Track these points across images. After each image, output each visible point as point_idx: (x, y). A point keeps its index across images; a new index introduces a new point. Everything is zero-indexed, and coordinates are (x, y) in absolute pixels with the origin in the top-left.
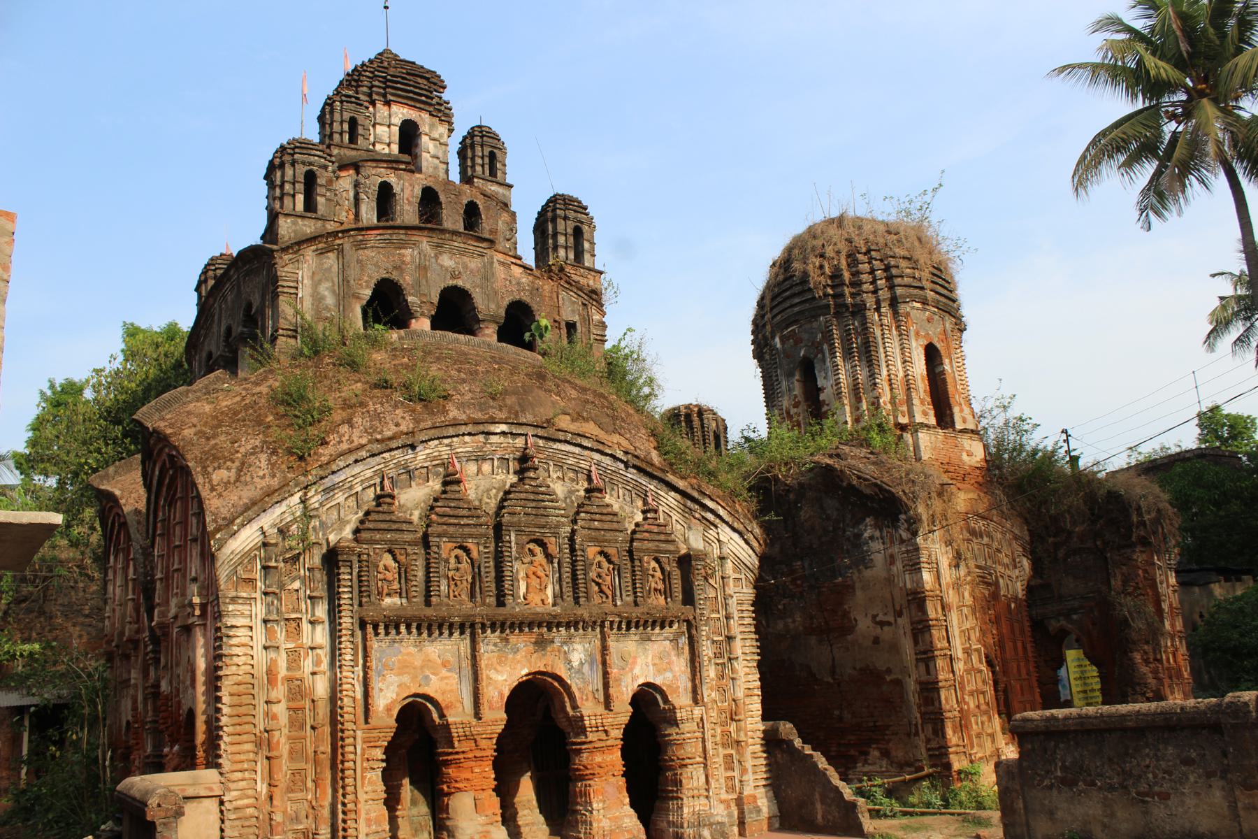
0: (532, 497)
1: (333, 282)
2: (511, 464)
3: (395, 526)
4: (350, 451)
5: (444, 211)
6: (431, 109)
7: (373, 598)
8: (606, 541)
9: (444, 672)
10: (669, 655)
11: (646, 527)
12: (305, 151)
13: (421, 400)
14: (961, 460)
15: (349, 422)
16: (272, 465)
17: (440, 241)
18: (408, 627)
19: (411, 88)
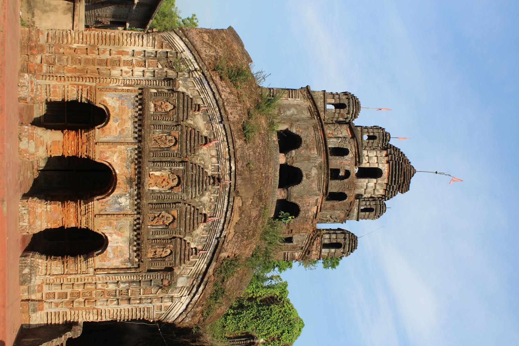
0: (201, 179)
1: (297, 115)
2: (216, 173)
3: (185, 109)
4: (218, 90)
5: (340, 181)
6: (390, 184)
7: (153, 97)
9: (119, 129)
10: (122, 256)
11: (187, 248)
12: (354, 104)
13: (244, 128)
15: (231, 93)
16: (211, 56)
17: (323, 168)
18: (140, 110)
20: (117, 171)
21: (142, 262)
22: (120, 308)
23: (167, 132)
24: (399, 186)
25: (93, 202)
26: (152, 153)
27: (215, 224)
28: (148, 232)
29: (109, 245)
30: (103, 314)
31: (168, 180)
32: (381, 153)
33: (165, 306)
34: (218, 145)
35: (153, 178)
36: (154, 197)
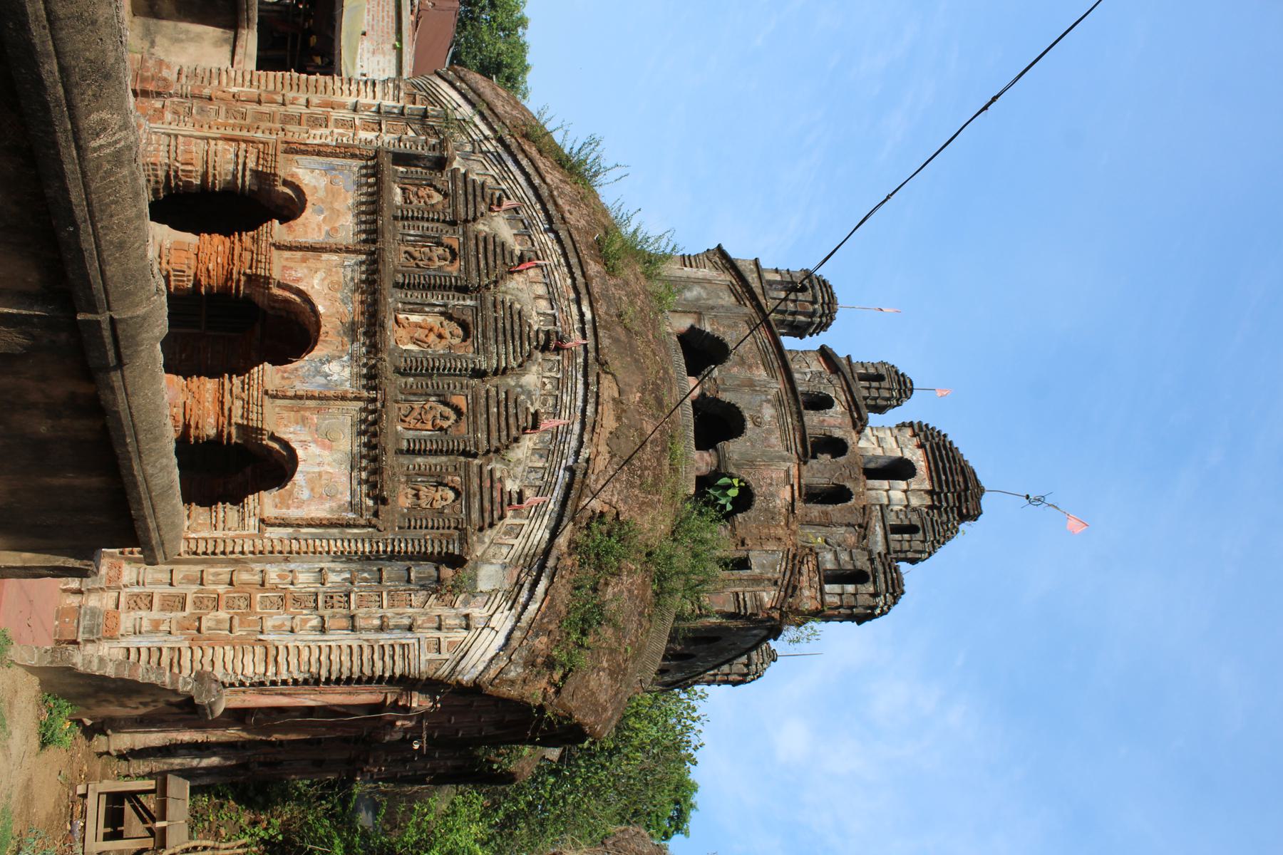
0: (516, 328)
1: (708, 299)
3: (470, 198)
4: (537, 169)
6: (937, 489)
9: (326, 228)
10: (331, 497)
11: (497, 485)
16: (517, 117)
17: (786, 402)
19: (948, 465)
20: (321, 309)
22: (329, 643)
23: (434, 237)
25: (261, 366)
26: (400, 275)
27: (559, 438)
28: (397, 440)
29: (299, 469)
30: (281, 659)
31: (441, 330)
32: (901, 433)
33: (450, 642)
35: (406, 325)
36: (409, 362)
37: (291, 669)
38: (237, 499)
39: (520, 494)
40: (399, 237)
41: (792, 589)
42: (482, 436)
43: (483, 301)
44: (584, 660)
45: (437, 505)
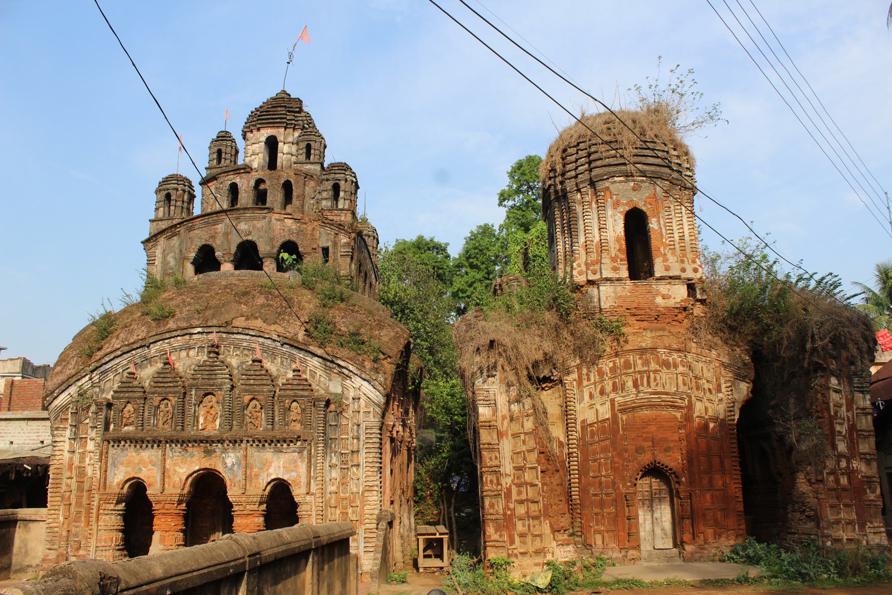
0: (208, 368)
3: (130, 389)
4: (111, 352)
6: (285, 125)
7: (116, 427)
8: (256, 392)
9: (150, 466)
10: (296, 461)
11: (290, 382)
14: (653, 304)
16: (76, 362)
18: (126, 442)
20: (197, 468)
21: (299, 437)
24: (289, 111)
26: (177, 428)
31: (209, 407)
34: (175, 349)
37: (375, 480)
38: (295, 505)
39: (294, 371)
40: (155, 428)
41: (340, 226)
42: (266, 388)
43: (191, 386)
44: (375, 343)
45: (300, 412)
